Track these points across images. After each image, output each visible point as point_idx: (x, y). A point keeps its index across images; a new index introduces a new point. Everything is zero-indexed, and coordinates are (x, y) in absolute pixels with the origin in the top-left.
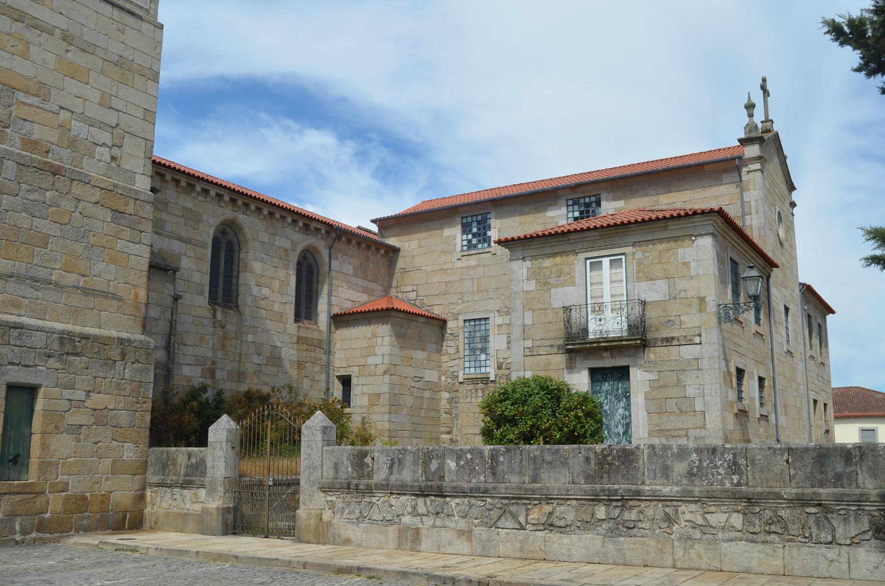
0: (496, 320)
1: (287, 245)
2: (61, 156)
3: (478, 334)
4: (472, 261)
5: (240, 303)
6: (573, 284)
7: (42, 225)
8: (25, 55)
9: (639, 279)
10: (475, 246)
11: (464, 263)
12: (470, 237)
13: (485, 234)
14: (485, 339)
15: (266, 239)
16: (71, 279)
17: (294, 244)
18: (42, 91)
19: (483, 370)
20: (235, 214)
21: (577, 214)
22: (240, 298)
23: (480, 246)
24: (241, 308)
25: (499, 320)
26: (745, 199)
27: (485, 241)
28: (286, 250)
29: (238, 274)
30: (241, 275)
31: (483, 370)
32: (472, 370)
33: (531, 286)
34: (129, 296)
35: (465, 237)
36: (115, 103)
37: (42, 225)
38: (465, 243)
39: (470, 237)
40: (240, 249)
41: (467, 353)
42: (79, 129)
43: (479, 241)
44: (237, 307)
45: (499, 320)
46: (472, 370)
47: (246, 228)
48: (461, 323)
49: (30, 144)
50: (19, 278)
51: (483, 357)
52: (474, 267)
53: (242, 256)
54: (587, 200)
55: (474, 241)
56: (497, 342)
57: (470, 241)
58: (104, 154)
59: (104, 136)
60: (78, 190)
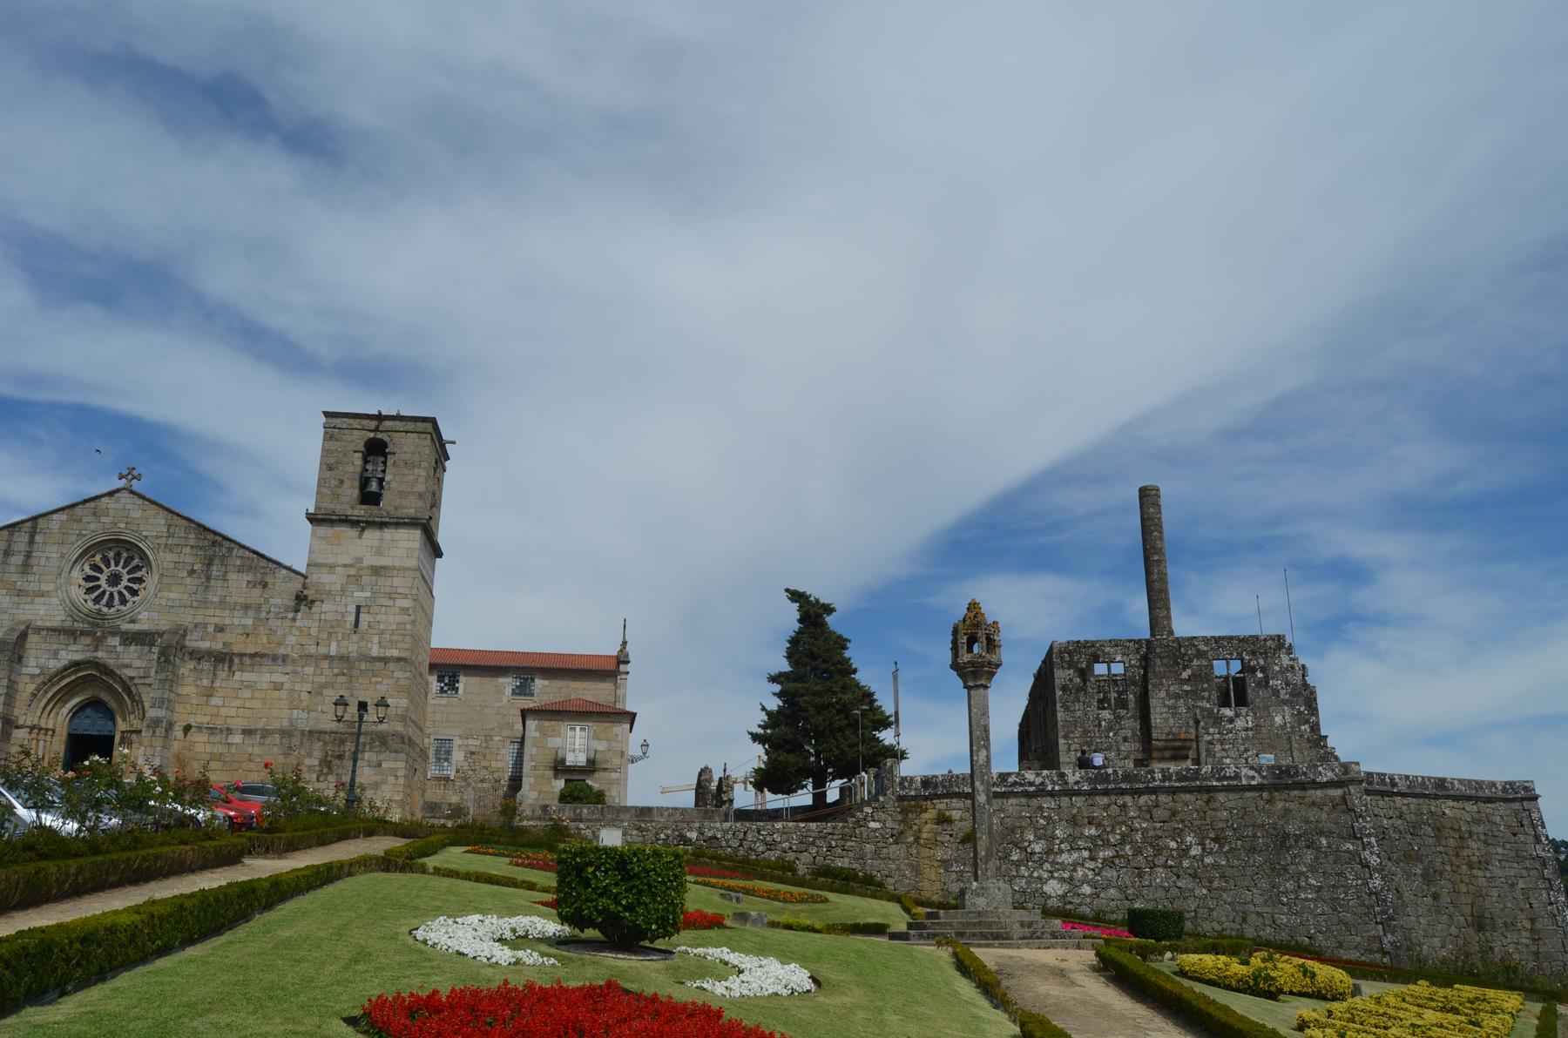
0: (457, 742)
3: (443, 749)
4: (444, 701)
6: (560, 736)
9: (593, 739)
10: (446, 692)
11: (437, 701)
12: (442, 685)
13: (454, 685)
14: (448, 753)
19: (445, 772)
21: (518, 684)
23: (449, 692)
25: (460, 742)
26: (618, 693)
27: (453, 689)
31: (445, 772)
32: (437, 772)
33: (537, 734)
35: (439, 684)
38: (439, 688)
39: (442, 685)
41: (434, 760)
43: (449, 689)
45: (460, 742)
46: (437, 772)
48: (432, 741)
51: (446, 764)
52: (444, 705)
54: (526, 676)
55: (446, 688)
56: (458, 756)
57: (442, 688)
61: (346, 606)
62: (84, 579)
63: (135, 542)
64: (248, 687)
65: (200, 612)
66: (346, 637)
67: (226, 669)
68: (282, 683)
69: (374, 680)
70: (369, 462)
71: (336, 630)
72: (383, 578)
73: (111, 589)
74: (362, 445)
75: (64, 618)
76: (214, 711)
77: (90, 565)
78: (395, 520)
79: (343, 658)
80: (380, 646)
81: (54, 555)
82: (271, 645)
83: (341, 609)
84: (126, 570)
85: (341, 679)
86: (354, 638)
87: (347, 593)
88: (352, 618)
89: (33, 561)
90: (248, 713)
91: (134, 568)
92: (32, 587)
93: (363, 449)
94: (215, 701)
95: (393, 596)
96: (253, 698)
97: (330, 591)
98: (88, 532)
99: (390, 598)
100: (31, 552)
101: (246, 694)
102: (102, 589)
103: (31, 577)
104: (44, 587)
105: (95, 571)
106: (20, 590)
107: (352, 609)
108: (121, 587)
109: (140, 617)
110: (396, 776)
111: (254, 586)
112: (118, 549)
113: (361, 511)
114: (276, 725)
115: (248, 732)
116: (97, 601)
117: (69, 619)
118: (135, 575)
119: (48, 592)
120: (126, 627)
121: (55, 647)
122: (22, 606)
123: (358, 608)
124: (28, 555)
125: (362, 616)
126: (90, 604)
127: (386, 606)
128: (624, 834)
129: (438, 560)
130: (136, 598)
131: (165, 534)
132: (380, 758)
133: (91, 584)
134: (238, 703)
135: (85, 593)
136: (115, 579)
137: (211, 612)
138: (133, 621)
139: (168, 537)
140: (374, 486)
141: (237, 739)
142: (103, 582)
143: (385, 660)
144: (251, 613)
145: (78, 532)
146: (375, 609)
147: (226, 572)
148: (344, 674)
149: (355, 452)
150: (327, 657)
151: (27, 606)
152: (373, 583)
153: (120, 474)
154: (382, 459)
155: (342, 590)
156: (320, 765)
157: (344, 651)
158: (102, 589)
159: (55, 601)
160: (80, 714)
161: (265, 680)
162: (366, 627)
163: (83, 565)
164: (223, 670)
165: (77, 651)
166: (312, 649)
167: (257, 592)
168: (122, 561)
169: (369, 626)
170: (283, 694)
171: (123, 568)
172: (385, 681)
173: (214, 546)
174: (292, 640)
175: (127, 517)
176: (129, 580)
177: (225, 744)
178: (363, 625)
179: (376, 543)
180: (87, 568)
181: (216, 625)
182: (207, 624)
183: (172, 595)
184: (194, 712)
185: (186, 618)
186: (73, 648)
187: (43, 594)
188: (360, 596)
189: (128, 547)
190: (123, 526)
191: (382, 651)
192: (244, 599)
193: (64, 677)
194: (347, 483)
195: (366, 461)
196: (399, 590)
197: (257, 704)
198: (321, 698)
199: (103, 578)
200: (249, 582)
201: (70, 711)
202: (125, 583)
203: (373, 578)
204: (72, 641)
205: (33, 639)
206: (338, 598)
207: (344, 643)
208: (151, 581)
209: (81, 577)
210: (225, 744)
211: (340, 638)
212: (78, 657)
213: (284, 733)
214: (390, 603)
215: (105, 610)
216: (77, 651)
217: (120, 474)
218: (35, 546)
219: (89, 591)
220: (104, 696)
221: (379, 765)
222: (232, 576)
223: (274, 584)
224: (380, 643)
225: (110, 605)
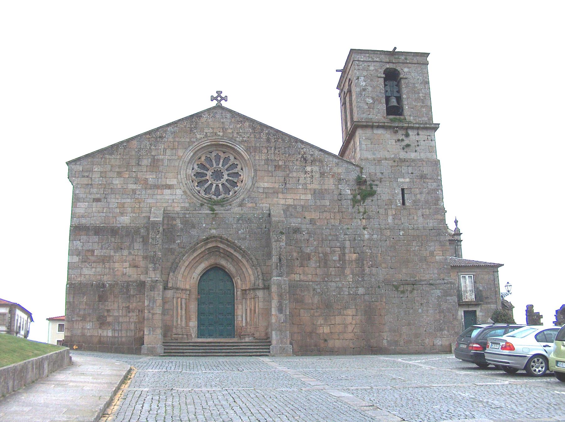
62: (194, 175)
63: (231, 145)
70: (387, 85)
74: (382, 73)
77: (198, 164)
93: (384, 76)
102: (210, 182)
104: (169, 182)
107: (398, 191)
108: (223, 180)
112: (217, 152)
116: (207, 191)
118: (233, 171)
123: (403, 190)
126: (203, 193)
130: (236, 189)
135: (197, 186)
136: (218, 175)
140: (393, 102)
151: (159, 197)
153: (212, 96)
154: (395, 83)
158: (210, 182)
159: (179, 192)
160: (205, 278)
163: (193, 165)
168: (222, 161)
180: (196, 167)
183: (266, 185)
187: (169, 187)
189: (224, 150)
195: (385, 85)
199: (209, 173)
202: (226, 177)
208: (246, 176)
209: (193, 174)
217: (212, 96)
219: (200, 183)
220: (223, 262)
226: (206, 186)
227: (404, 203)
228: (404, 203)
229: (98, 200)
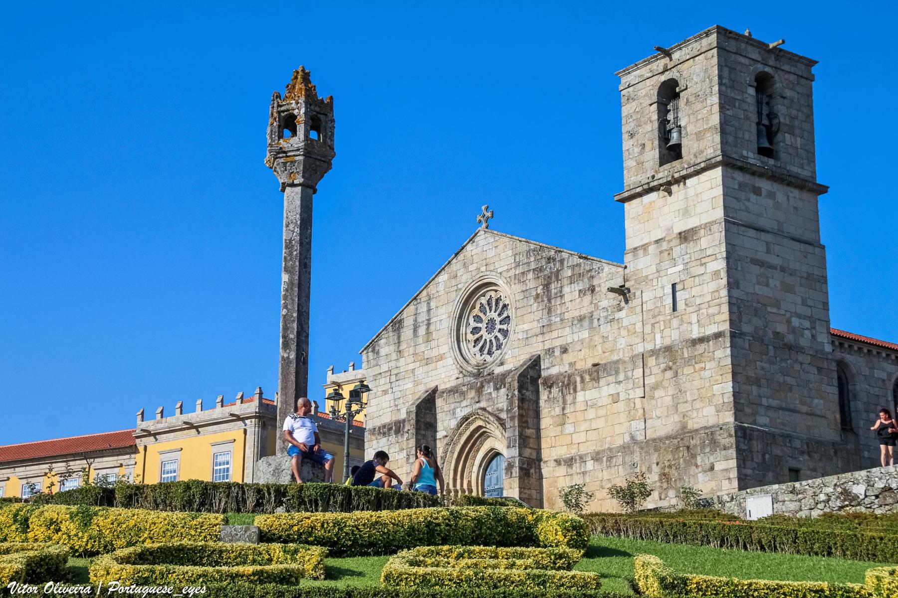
1: (884, 376)
2: (790, 338)
5: (853, 426)
7: (789, 380)
8: (767, 285)
15: (867, 373)
16: (805, 409)
17: (889, 375)
18: (777, 304)
20: (843, 355)
22: (854, 422)
24: (855, 430)
28: (883, 381)
29: (849, 402)
30: (852, 403)
34: (831, 417)
36: (810, 302)
37: (789, 380)
40: (848, 383)
42: (795, 322)
44: (852, 429)
47: (852, 366)
49: (776, 334)
50: (782, 409)
53: (850, 388)
58: (807, 333)
59: (807, 324)
60: (801, 358)
61: (663, 288)
64: (592, 407)
65: (547, 337)
66: (668, 324)
67: (572, 391)
68: (618, 394)
69: (697, 366)
71: (657, 319)
72: (691, 243)
73: (490, 336)
75: (457, 376)
76: (568, 441)
78: (692, 169)
79: (668, 349)
80: (699, 325)
81: (444, 317)
82: (606, 354)
83: (659, 293)
84: (497, 313)
85: (669, 374)
86: (675, 323)
87: (662, 273)
88: (670, 300)
89: (432, 328)
90: (593, 435)
91: (503, 308)
92: (435, 353)
94: (569, 428)
95: (704, 261)
96: (597, 417)
97: (647, 277)
98: (462, 285)
99: (702, 265)
100: (429, 320)
101: (591, 414)
103: (433, 344)
105: (477, 322)
106: (428, 359)
109: (506, 357)
110: (729, 479)
111: (584, 295)
113: (665, 173)
114: (619, 442)
115: (597, 457)
117: (461, 375)
119: (444, 354)
120: (498, 370)
121: (452, 406)
122: (430, 374)
123: (674, 286)
124: (429, 325)
125: (678, 294)
126: (478, 355)
127: (699, 275)
128: (775, 501)
129: (820, 198)
131: (513, 265)
132: (712, 459)
133: (477, 336)
134: (584, 426)
137: (554, 334)
138: (502, 364)
139: (515, 268)
141: (590, 465)
142: (483, 332)
143: (702, 340)
144: (586, 323)
145: (455, 288)
146: (689, 283)
147: (561, 287)
148: (670, 368)
149: (651, 105)
150: (654, 353)
151: (434, 373)
152: (683, 252)
155: (658, 271)
156: (660, 480)
157: (667, 342)
161: (604, 395)
162: (683, 307)
164: (569, 394)
165: (467, 406)
166: (639, 349)
167: (587, 298)
169: (686, 305)
170: (621, 406)
171: (495, 312)
172: (708, 365)
173: (549, 263)
174: (622, 343)
175: (486, 259)
176: (501, 322)
177: (580, 473)
178: (681, 305)
179: (681, 205)
181: (561, 347)
182: (553, 348)
183: (526, 327)
184: (553, 445)
185: (536, 348)
186: (464, 404)
188: (674, 272)
190: (483, 269)
191: (702, 330)
192: (578, 311)
193: (461, 434)
194: (648, 148)
196: (709, 252)
197: (600, 423)
198: (653, 402)
199: (483, 326)
200: (580, 291)
201: (480, 466)
202: (498, 326)
203: (683, 246)
204: (463, 398)
205: (439, 402)
206: (655, 283)
207: (667, 332)
210: (580, 473)
211: (662, 328)
212: (466, 412)
213: (625, 449)
214: (701, 270)
215: (489, 359)
216: (467, 406)
218: (432, 312)
221: (712, 468)
222: (566, 290)
223: (599, 286)
224: (698, 321)
225: (490, 353)
226: (480, 345)
227: (674, 309)
228: (674, 309)
229: (385, 392)
